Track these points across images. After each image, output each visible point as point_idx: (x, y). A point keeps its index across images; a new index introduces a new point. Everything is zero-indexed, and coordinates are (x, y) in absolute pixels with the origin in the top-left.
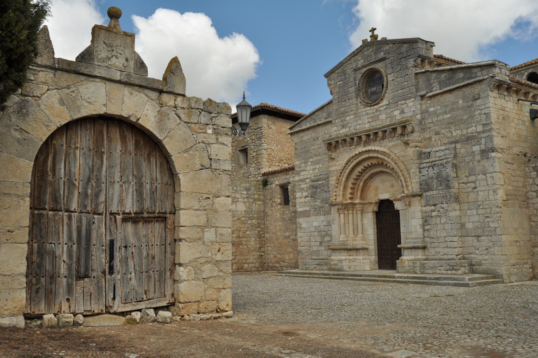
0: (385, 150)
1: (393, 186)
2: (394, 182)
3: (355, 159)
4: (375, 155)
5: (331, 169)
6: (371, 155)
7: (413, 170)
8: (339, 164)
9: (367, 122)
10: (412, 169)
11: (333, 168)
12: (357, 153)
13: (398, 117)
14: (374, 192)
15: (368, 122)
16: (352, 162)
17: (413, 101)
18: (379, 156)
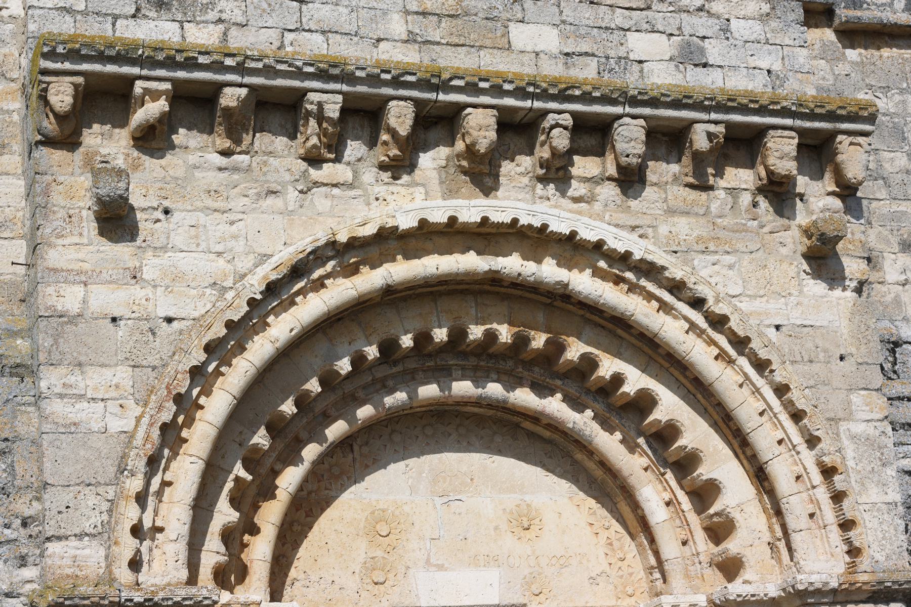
0: (659, 257)
1: (525, 523)
2: (539, 500)
3: (352, 271)
4: (549, 271)
5: (69, 298)
6: (512, 264)
7: (859, 428)
8: (175, 280)
9: (397, 26)
10: (849, 417)
11: (106, 298)
12: (406, 222)
13: (662, 76)
14: (361, 550)
15: (411, 39)
16: (319, 285)
17: (764, 18)
18: (584, 282)
